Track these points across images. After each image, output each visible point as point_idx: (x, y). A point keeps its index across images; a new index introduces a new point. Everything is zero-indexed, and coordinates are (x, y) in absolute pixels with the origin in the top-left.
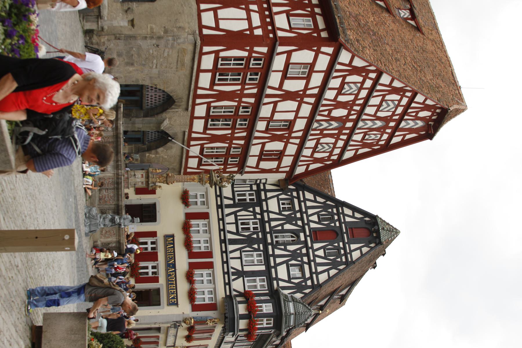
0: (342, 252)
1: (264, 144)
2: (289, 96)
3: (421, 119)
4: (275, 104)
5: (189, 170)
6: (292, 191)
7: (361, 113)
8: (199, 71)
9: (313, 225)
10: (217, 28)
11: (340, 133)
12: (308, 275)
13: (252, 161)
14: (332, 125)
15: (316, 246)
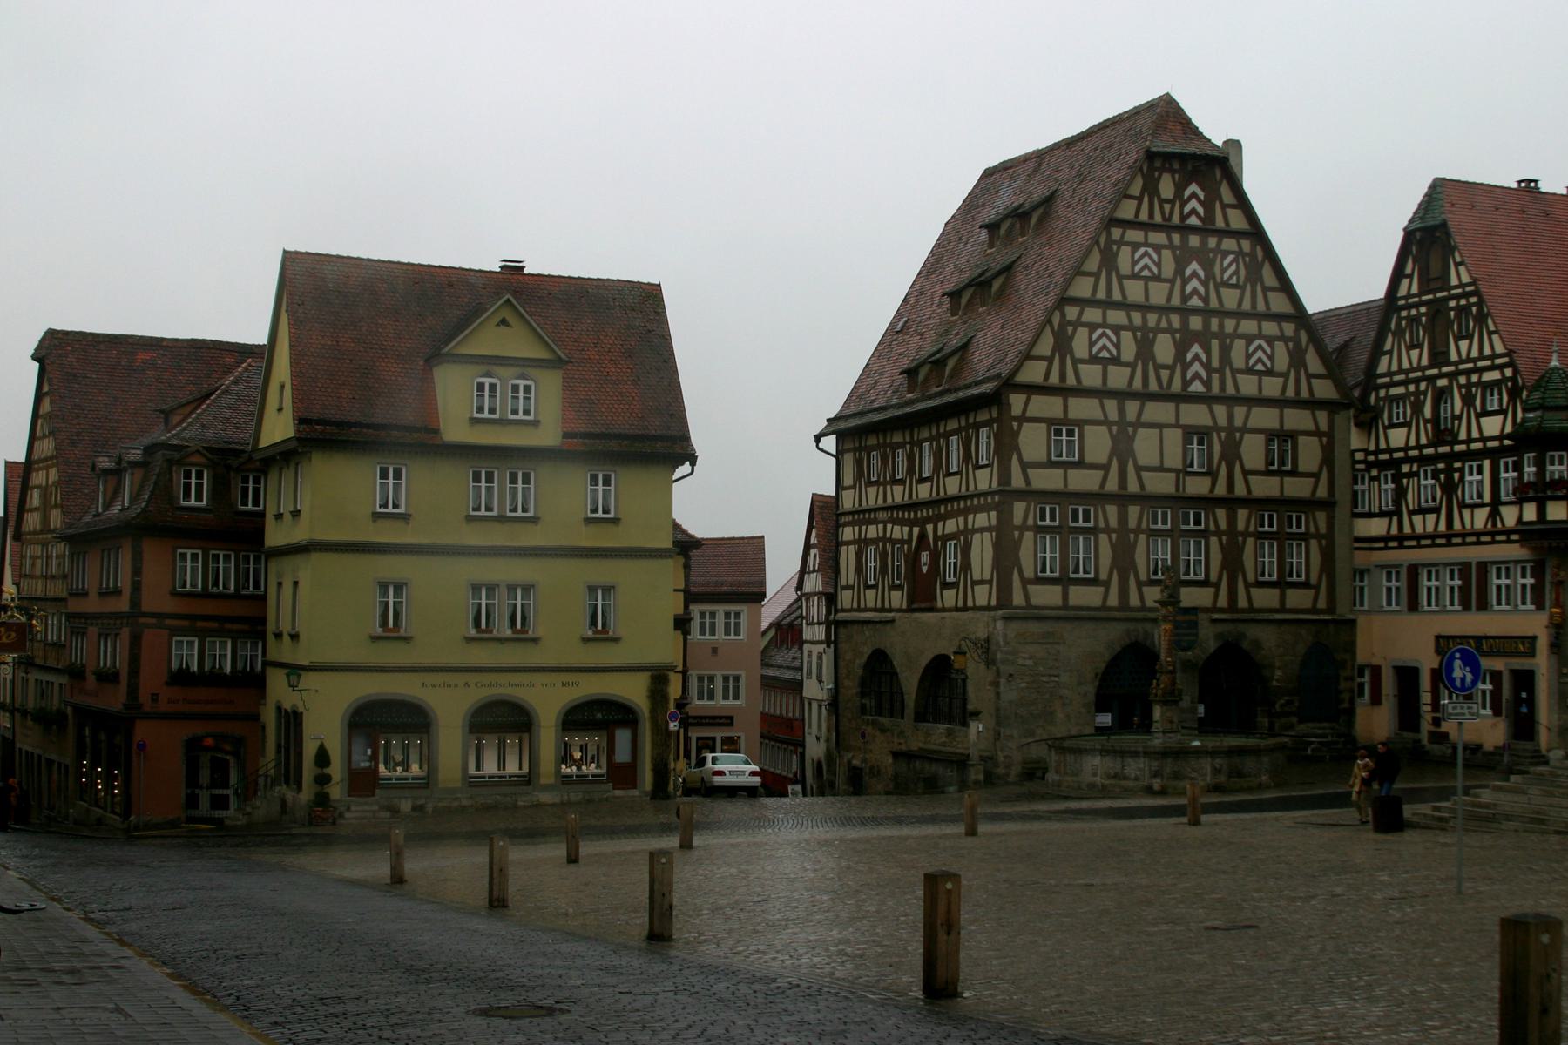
0: (1463, 302)
1: (1246, 473)
2: (1122, 449)
3: (1180, 189)
4: (1139, 469)
5: (1322, 604)
6: (1378, 398)
7: (1164, 310)
8: (1065, 607)
9: (1425, 362)
10: (990, 582)
11: (1221, 335)
12: (1495, 375)
13: (1297, 488)
14: (1196, 358)
15: (1454, 356)
